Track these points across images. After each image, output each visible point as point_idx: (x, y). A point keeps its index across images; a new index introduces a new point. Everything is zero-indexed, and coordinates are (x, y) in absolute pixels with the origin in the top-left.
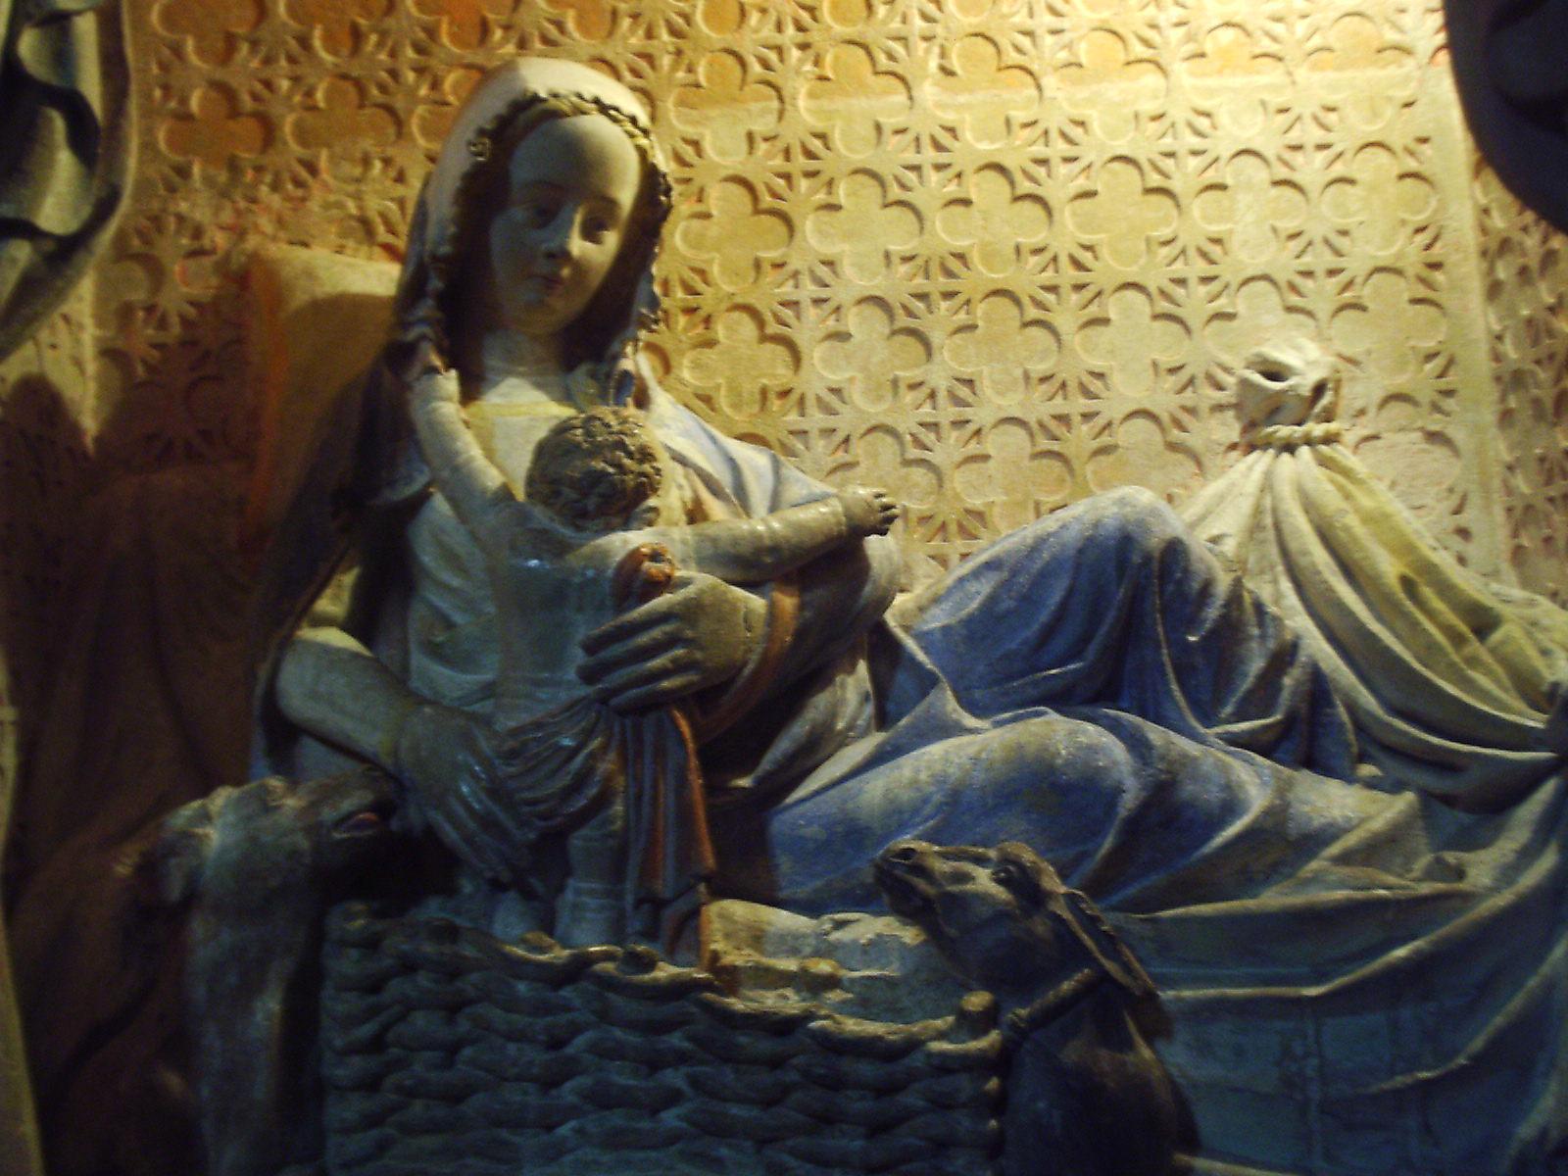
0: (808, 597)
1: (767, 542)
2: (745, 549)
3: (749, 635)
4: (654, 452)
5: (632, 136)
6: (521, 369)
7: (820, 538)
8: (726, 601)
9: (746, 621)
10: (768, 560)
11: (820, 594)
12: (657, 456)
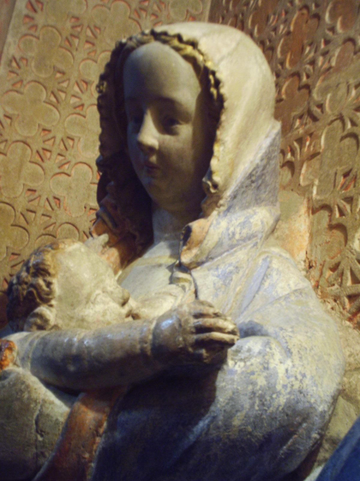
0: (123, 417)
1: (74, 351)
2: (58, 355)
3: (40, 438)
4: (46, 268)
5: (177, 49)
6: (166, 235)
7: (119, 354)
8: (20, 400)
9: (37, 423)
10: (72, 368)
11: (135, 417)
12: (51, 271)
